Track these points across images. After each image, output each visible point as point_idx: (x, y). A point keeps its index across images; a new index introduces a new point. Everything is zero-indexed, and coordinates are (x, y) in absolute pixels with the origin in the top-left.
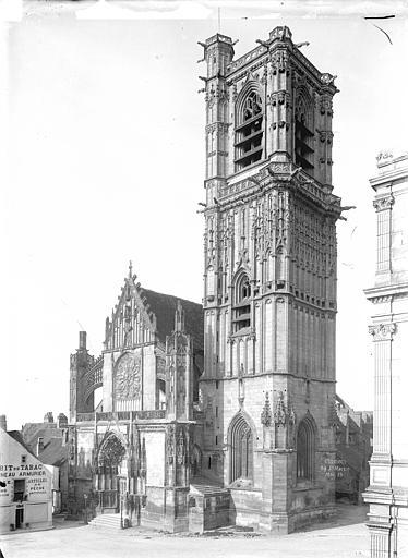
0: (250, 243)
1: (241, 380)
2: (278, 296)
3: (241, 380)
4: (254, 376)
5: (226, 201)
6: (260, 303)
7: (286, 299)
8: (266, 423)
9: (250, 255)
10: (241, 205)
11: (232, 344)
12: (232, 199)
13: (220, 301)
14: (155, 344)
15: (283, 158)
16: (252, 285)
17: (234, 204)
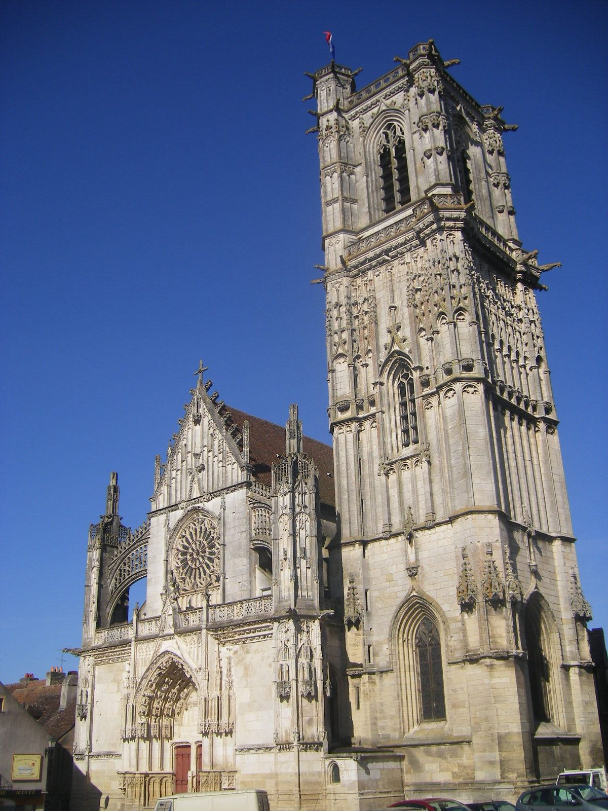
0: (405, 313)
1: (410, 538)
2: (464, 383)
3: (410, 538)
4: (431, 525)
5: (362, 259)
6: (434, 400)
7: (481, 387)
8: (467, 607)
9: (406, 331)
10: (385, 261)
11: (387, 475)
12: (371, 254)
13: (360, 407)
14: (249, 485)
15: (448, 190)
16: (416, 375)
17: (374, 263)
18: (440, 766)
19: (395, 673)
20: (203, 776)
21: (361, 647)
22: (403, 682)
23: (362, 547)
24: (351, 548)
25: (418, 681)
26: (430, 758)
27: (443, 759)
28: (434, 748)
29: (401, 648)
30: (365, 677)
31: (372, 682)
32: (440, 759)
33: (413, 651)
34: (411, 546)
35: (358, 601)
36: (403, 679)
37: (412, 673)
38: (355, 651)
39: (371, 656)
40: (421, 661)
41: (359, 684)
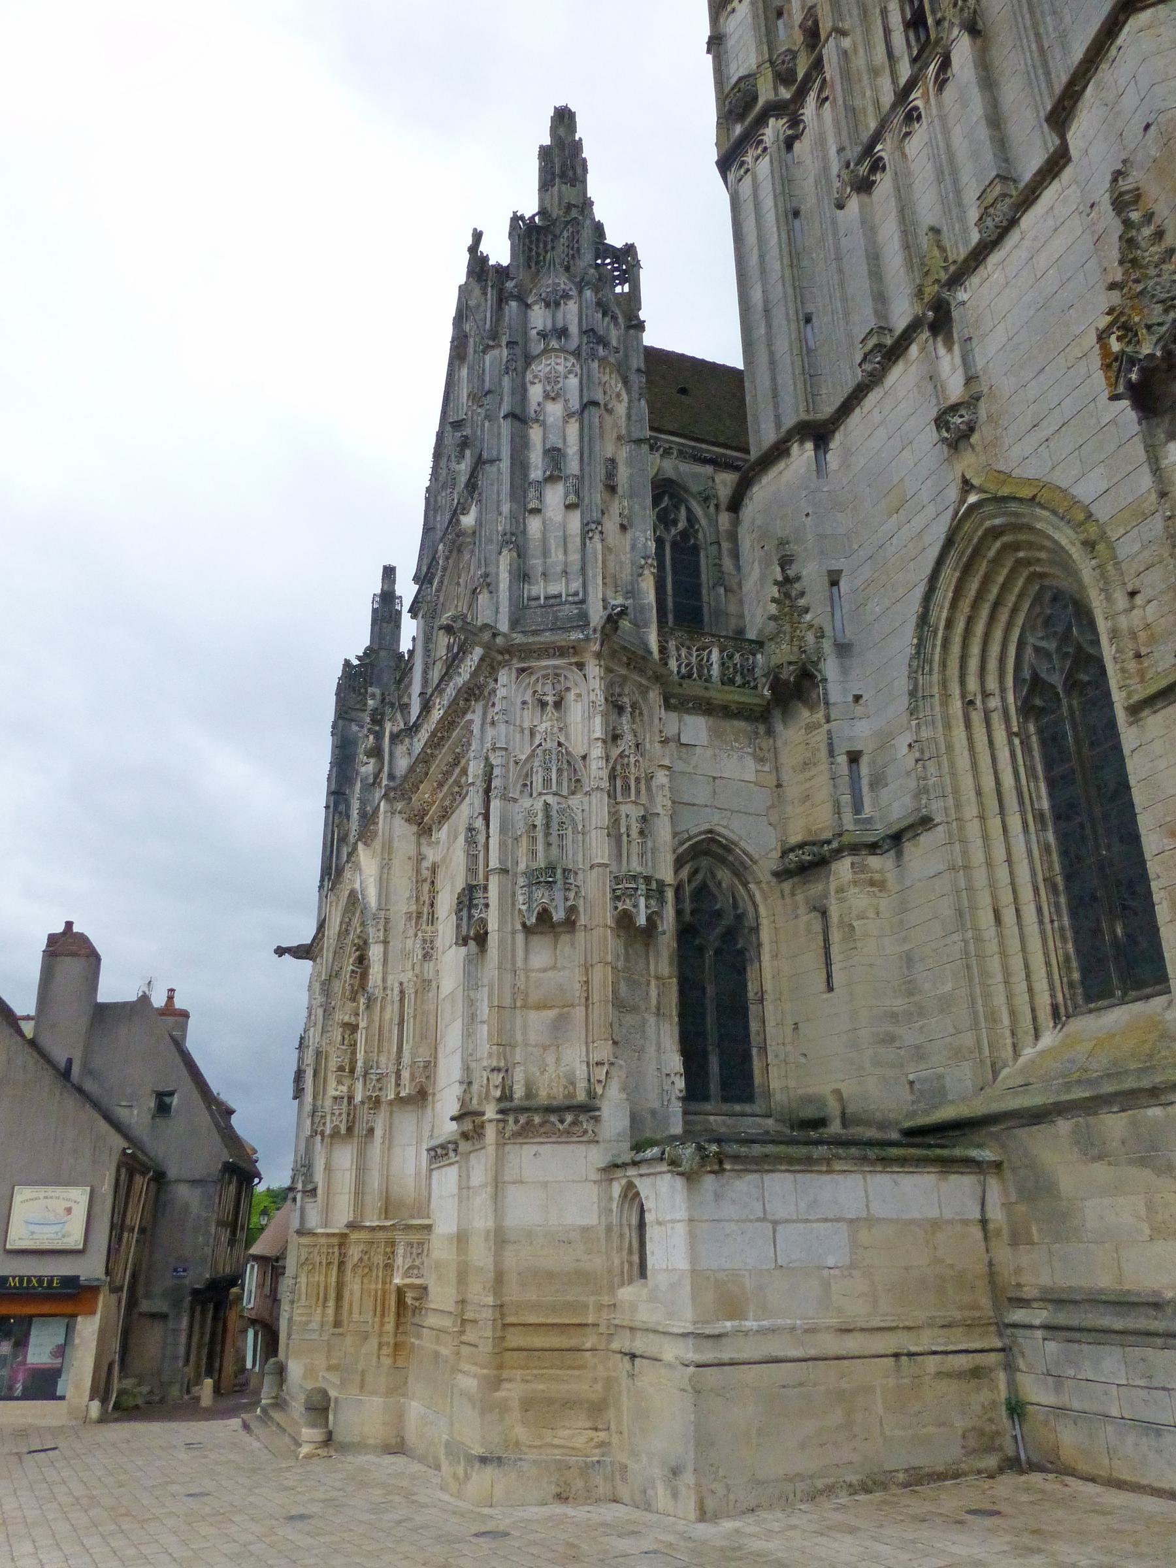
18: (1149, 1206)
19: (940, 828)
20: (358, 1242)
21: (823, 766)
22: (978, 857)
23: (809, 446)
24: (781, 465)
25: (1047, 849)
26: (1101, 1171)
27: (1159, 1172)
28: (1114, 1124)
29: (959, 733)
30: (843, 868)
31: (872, 883)
32: (1146, 1174)
33: (1010, 734)
34: (950, 349)
35: (808, 617)
36: (976, 845)
37: (1015, 822)
38: (808, 785)
39: (865, 789)
40: (1049, 766)
41: (826, 895)
